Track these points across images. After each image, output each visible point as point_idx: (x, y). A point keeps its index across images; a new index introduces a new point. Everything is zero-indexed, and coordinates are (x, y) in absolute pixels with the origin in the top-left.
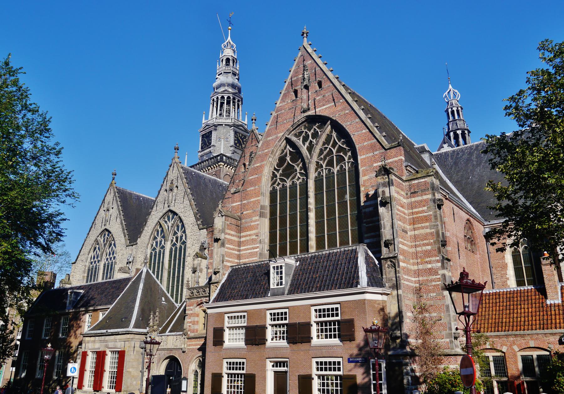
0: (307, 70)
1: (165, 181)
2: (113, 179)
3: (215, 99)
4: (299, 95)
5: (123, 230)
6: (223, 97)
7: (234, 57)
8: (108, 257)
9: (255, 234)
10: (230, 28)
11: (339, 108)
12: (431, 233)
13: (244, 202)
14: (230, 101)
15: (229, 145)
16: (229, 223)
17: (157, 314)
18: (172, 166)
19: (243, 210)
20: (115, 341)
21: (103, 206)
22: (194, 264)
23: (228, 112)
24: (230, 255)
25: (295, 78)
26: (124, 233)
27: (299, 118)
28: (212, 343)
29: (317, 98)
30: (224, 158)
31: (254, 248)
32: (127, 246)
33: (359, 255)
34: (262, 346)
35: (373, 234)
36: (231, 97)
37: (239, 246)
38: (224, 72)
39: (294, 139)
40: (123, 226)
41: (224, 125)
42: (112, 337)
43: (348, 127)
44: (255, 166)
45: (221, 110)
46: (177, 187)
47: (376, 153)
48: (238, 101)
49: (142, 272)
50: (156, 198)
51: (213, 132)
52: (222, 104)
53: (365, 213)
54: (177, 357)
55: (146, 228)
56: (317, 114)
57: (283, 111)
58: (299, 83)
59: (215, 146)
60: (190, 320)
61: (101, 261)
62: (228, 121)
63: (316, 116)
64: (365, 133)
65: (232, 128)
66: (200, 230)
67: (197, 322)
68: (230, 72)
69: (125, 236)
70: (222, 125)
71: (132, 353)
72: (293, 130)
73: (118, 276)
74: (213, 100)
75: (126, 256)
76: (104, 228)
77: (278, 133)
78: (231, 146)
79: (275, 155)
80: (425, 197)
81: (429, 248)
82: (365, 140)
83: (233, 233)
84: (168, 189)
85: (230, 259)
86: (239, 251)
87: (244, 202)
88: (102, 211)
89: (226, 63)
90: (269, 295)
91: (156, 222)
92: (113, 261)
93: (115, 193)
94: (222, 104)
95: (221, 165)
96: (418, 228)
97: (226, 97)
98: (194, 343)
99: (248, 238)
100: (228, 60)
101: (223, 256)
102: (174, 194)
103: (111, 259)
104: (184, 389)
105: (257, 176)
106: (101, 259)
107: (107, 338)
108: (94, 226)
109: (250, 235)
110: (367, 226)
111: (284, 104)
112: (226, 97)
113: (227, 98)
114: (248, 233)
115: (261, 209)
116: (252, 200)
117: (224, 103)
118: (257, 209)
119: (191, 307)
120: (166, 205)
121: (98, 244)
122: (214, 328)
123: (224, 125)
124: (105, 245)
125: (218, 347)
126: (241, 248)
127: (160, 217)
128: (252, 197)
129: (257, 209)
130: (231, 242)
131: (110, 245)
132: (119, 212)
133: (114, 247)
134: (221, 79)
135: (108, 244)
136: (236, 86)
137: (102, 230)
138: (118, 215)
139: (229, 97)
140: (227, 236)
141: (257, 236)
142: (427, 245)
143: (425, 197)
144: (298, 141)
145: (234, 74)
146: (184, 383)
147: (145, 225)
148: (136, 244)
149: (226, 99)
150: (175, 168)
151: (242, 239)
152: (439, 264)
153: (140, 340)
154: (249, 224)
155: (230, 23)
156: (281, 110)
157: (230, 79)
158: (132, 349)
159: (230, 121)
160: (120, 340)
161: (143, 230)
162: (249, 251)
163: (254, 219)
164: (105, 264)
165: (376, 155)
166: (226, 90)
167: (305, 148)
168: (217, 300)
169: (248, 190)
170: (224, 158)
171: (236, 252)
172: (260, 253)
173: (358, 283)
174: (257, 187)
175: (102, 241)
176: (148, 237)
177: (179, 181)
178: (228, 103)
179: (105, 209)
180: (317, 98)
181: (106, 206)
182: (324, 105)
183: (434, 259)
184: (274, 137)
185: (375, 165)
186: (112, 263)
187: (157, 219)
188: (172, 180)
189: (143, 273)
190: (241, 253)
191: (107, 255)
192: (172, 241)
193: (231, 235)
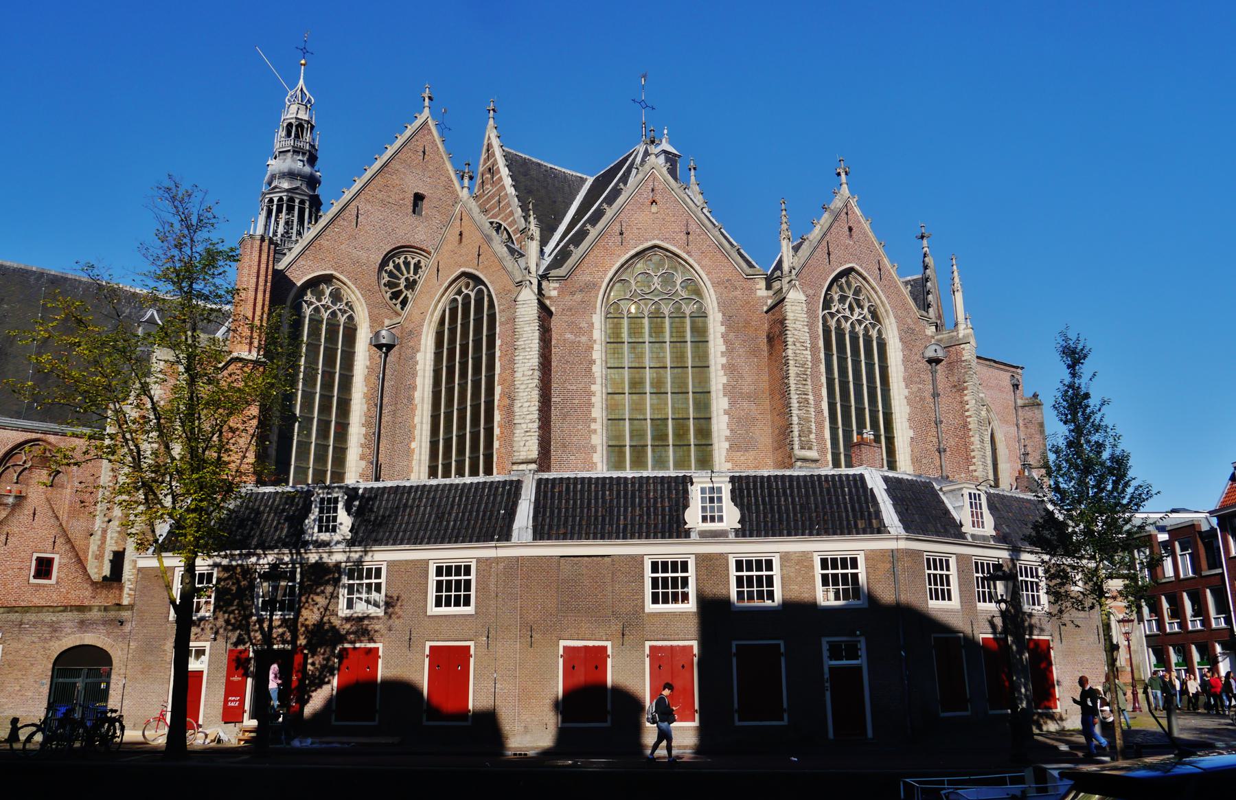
7: (302, 119)
10: (303, 62)
14: (282, 205)
36: (285, 198)
38: (280, 152)
48: (302, 202)
68: (289, 151)
97: (276, 200)
100: (290, 125)
112: (276, 200)
113: (278, 201)
134: (276, 165)
136: (299, 175)
139: (281, 199)
145: (296, 151)
149: (275, 202)
155: (304, 52)
157: (298, 165)
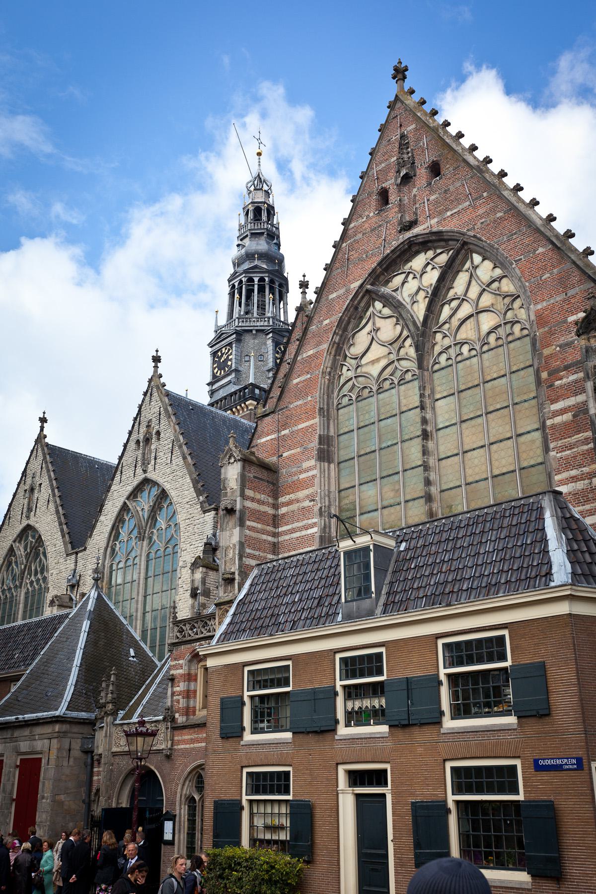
0: (408, 143)
1: (137, 424)
2: (42, 428)
3: (236, 284)
4: (393, 198)
5: (60, 524)
6: (251, 280)
8: (33, 578)
9: (307, 497)
11: (481, 211)
13: (283, 433)
15: (266, 368)
16: (252, 476)
17: (113, 678)
18: (149, 394)
19: (282, 449)
20: (32, 738)
21: (23, 482)
22: (193, 581)
23: (262, 307)
24: (257, 544)
25: (383, 165)
26: (62, 531)
27: (395, 244)
28: (218, 731)
29: (432, 198)
30: (257, 391)
31: (306, 528)
32: (67, 555)
33: (548, 515)
34: (328, 736)
35: (574, 473)
36: (267, 279)
37: (276, 525)
38: (252, 234)
39: (386, 290)
40: (59, 518)
41: (254, 332)
42: (26, 732)
43: (503, 247)
44: (305, 355)
45: (247, 305)
46: (158, 433)
47: (571, 292)
48: (281, 285)
49: (89, 598)
50: (121, 458)
51: (234, 345)
52: (250, 292)
53: (553, 427)
54: (153, 768)
55: (102, 518)
56: (434, 230)
57: (360, 236)
58: (392, 174)
59: (239, 371)
61: (21, 588)
62: (262, 324)
63: (432, 233)
64: (543, 254)
65: (271, 335)
66: (205, 512)
67: (195, 691)
68: (263, 233)
69: (63, 536)
70: (251, 331)
71: (65, 764)
72: (382, 274)
73: (49, 612)
74: (234, 286)
75: (67, 574)
76: (25, 523)
77: (350, 282)
78: (269, 371)
79: (345, 330)
82: (544, 269)
83: (263, 497)
84: (141, 437)
85: (257, 553)
86: (275, 535)
87: (283, 433)
88: (21, 492)
89: (255, 216)
90: (340, 618)
91: (119, 504)
92: (43, 586)
93: (44, 454)
94: (250, 292)
95: (251, 404)
97: (256, 280)
98: (186, 737)
99: (294, 507)
100: (258, 211)
101: (242, 544)
102: (153, 447)
103: (38, 581)
104: (168, 836)
105: (309, 376)
106: (21, 583)
107: (17, 733)
108: (7, 521)
109: (298, 501)
110: (559, 455)
111: (361, 221)
112: (256, 280)
113: (259, 281)
114: (292, 496)
115: (320, 443)
116: (300, 426)
117: (253, 290)
118: (312, 445)
119: (181, 662)
120: (139, 470)
121: (15, 555)
122: (222, 699)
123: (254, 332)
124: (27, 556)
125: (229, 744)
127: (127, 494)
128: (301, 420)
129: (312, 445)
130: (259, 516)
131: (37, 555)
132: (53, 490)
133: (42, 558)
135: (32, 553)
137: (21, 527)
138: (51, 498)
139: (262, 280)
140: (248, 504)
141: (313, 500)
144: (394, 293)
146: (168, 826)
147: (100, 511)
148: (85, 549)
149: (256, 282)
150: (155, 394)
151: (283, 510)
153: (80, 736)
154: (296, 478)
156: (355, 235)
158: (65, 754)
159: (266, 324)
160: (42, 737)
161: (97, 521)
162: (298, 534)
163: (306, 465)
164: (27, 593)
165: (574, 297)
166: (256, 267)
168: (227, 636)
169: (291, 406)
170: (257, 391)
171: (270, 539)
172: (321, 537)
173: (549, 574)
174: (309, 398)
175: (22, 550)
176: (107, 535)
177: (162, 421)
178: (261, 290)
179: (27, 487)
180: (432, 198)
181: (29, 481)
184: (341, 292)
185: (571, 319)
186: (40, 589)
187: (122, 499)
188: (150, 421)
189: (91, 600)
190: (281, 539)
191: (31, 576)
192: (150, 538)
193: (259, 502)
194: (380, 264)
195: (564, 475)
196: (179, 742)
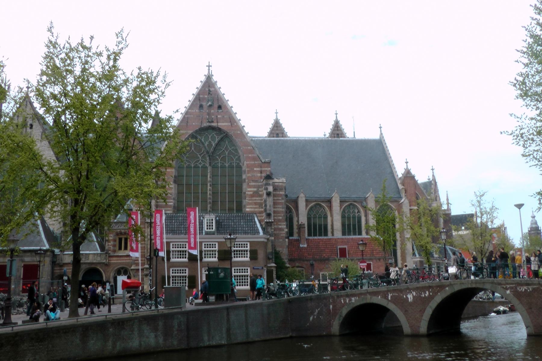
12: (282, 211)
53: (247, 194)
56: (219, 127)
60: (110, 244)
63: (218, 127)
80: (281, 193)
81: (281, 218)
96: (276, 208)
126: (158, 201)
142: (280, 216)
143: (281, 193)
152: (285, 226)
167: (206, 145)
182: (223, 123)
183: (282, 223)
194: (199, 129)
195: (249, 206)
196: (111, 260)
